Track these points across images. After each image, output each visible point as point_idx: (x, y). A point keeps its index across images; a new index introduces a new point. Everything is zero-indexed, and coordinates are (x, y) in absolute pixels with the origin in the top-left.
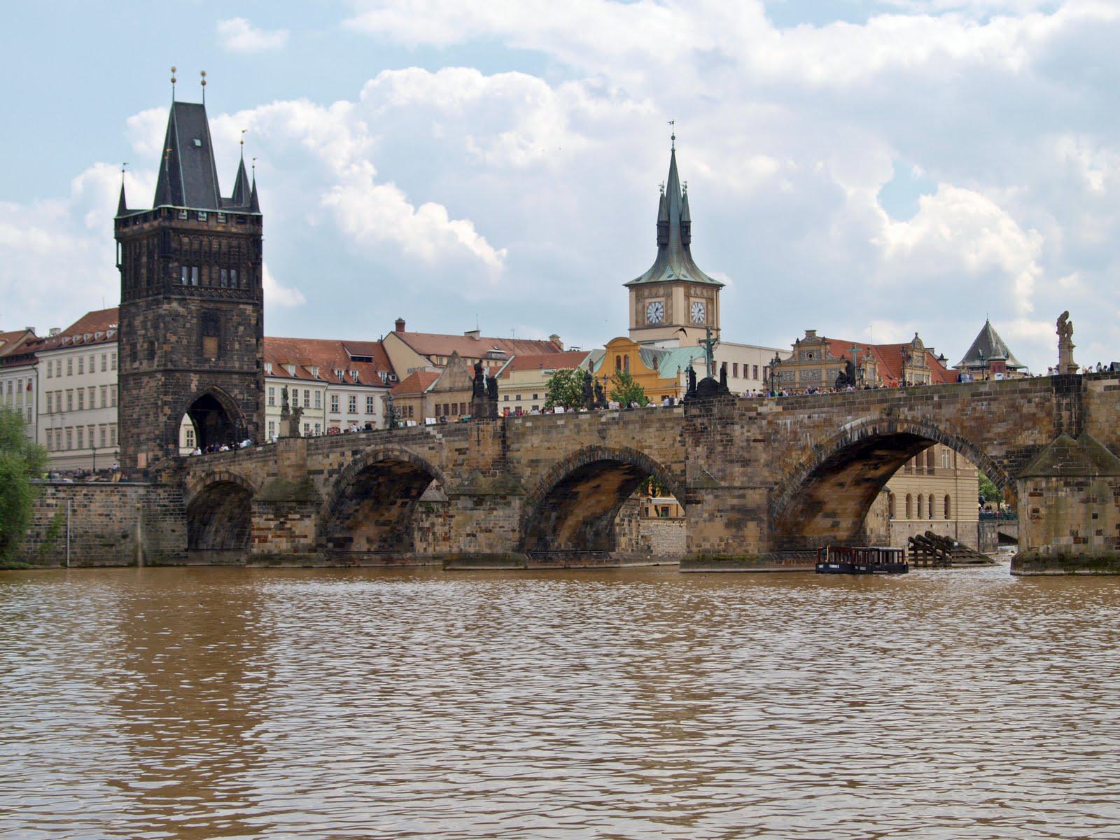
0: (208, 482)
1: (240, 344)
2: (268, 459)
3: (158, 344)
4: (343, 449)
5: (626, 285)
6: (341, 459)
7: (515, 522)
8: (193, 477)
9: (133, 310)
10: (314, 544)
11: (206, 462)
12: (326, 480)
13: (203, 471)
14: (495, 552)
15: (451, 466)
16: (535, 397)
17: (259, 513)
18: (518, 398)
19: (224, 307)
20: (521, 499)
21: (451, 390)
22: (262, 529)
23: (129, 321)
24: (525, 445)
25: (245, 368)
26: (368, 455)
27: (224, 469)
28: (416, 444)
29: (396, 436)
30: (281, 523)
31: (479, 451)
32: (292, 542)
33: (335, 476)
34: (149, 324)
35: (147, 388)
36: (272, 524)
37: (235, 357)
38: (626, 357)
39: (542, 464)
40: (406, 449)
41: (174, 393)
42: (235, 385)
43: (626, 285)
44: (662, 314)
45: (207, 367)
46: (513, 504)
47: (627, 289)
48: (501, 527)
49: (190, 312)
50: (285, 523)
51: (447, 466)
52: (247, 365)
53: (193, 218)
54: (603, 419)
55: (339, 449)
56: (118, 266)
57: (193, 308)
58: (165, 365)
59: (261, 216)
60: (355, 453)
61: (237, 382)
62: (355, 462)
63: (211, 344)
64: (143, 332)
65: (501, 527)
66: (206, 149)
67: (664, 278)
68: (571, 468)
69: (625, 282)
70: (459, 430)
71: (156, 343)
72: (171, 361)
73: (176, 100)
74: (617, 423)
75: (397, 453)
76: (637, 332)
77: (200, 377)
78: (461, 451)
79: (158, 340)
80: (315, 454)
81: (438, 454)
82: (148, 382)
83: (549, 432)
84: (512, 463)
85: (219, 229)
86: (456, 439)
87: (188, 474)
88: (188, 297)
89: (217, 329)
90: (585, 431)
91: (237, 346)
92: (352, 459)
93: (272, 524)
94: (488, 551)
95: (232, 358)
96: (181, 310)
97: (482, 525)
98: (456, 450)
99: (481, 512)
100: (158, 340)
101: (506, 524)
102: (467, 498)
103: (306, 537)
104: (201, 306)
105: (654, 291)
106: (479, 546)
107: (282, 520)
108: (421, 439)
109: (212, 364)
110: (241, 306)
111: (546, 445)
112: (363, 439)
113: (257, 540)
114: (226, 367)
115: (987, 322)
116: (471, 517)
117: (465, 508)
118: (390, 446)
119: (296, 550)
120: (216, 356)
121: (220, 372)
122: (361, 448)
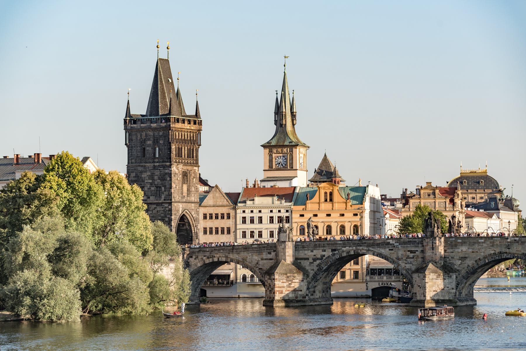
0: (207, 261)
1: (194, 188)
2: (262, 251)
3: (165, 188)
4: (325, 248)
5: (262, 146)
6: (324, 253)
7: (454, 285)
8: (195, 259)
9: (140, 169)
10: (305, 294)
11: (209, 251)
12: (311, 263)
13: (204, 256)
14: (445, 299)
15: (404, 258)
16: (271, 211)
17: (279, 279)
18: (260, 211)
19: (189, 168)
20: (456, 274)
21: (214, 206)
22: (281, 287)
23: (136, 174)
24: (457, 250)
25: (196, 201)
26: (343, 251)
27: (224, 256)
28: (380, 247)
29: (365, 243)
30: (289, 284)
31: (433, 253)
32: (295, 293)
33: (318, 262)
34: (156, 177)
35: (154, 211)
36: (285, 285)
37: (193, 196)
38: (331, 194)
39: (468, 259)
40: (372, 249)
41: (175, 214)
42: (193, 210)
43: (262, 146)
44: (285, 163)
45: (184, 201)
46: (452, 277)
47: (262, 148)
48: (448, 287)
49: (179, 172)
50: (291, 284)
51: (402, 258)
52: (197, 199)
53: (180, 123)
54: (509, 240)
55: (322, 248)
56: (126, 144)
57: (180, 169)
58: (171, 200)
59: (201, 121)
60: (333, 250)
61: (193, 208)
62: (334, 255)
63: (185, 187)
64: (151, 181)
65: (448, 287)
66: (172, 83)
67: (287, 143)
68: (487, 261)
69: (262, 144)
70: (411, 241)
71: (163, 188)
72: (174, 198)
73: (160, 57)
74: (518, 242)
75: (365, 251)
76: (270, 172)
77: (182, 206)
78: (411, 252)
79: (165, 186)
80: (301, 250)
81: (395, 253)
82: (156, 208)
83: (473, 245)
84: (448, 258)
85: (188, 128)
86: (409, 246)
87: (192, 257)
88: (179, 164)
89: (187, 181)
90: (497, 245)
91: (193, 189)
92: (332, 253)
93: (285, 285)
94: (442, 298)
95: (192, 195)
96: (177, 171)
97: (440, 287)
98: (409, 251)
99: (440, 280)
100: (165, 186)
101: (449, 286)
102: (434, 274)
103: (301, 291)
104: (182, 169)
105: (280, 150)
106: (439, 296)
107: (290, 282)
108: (384, 245)
109: (186, 199)
110: (195, 168)
111: (471, 250)
112: (340, 244)
113: (278, 292)
114: (190, 200)
115: (325, 154)
116: (435, 283)
117: (432, 279)
118: (358, 248)
119: (296, 297)
120: (186, 194)
121: (189, 202)
122: (339, 248)
